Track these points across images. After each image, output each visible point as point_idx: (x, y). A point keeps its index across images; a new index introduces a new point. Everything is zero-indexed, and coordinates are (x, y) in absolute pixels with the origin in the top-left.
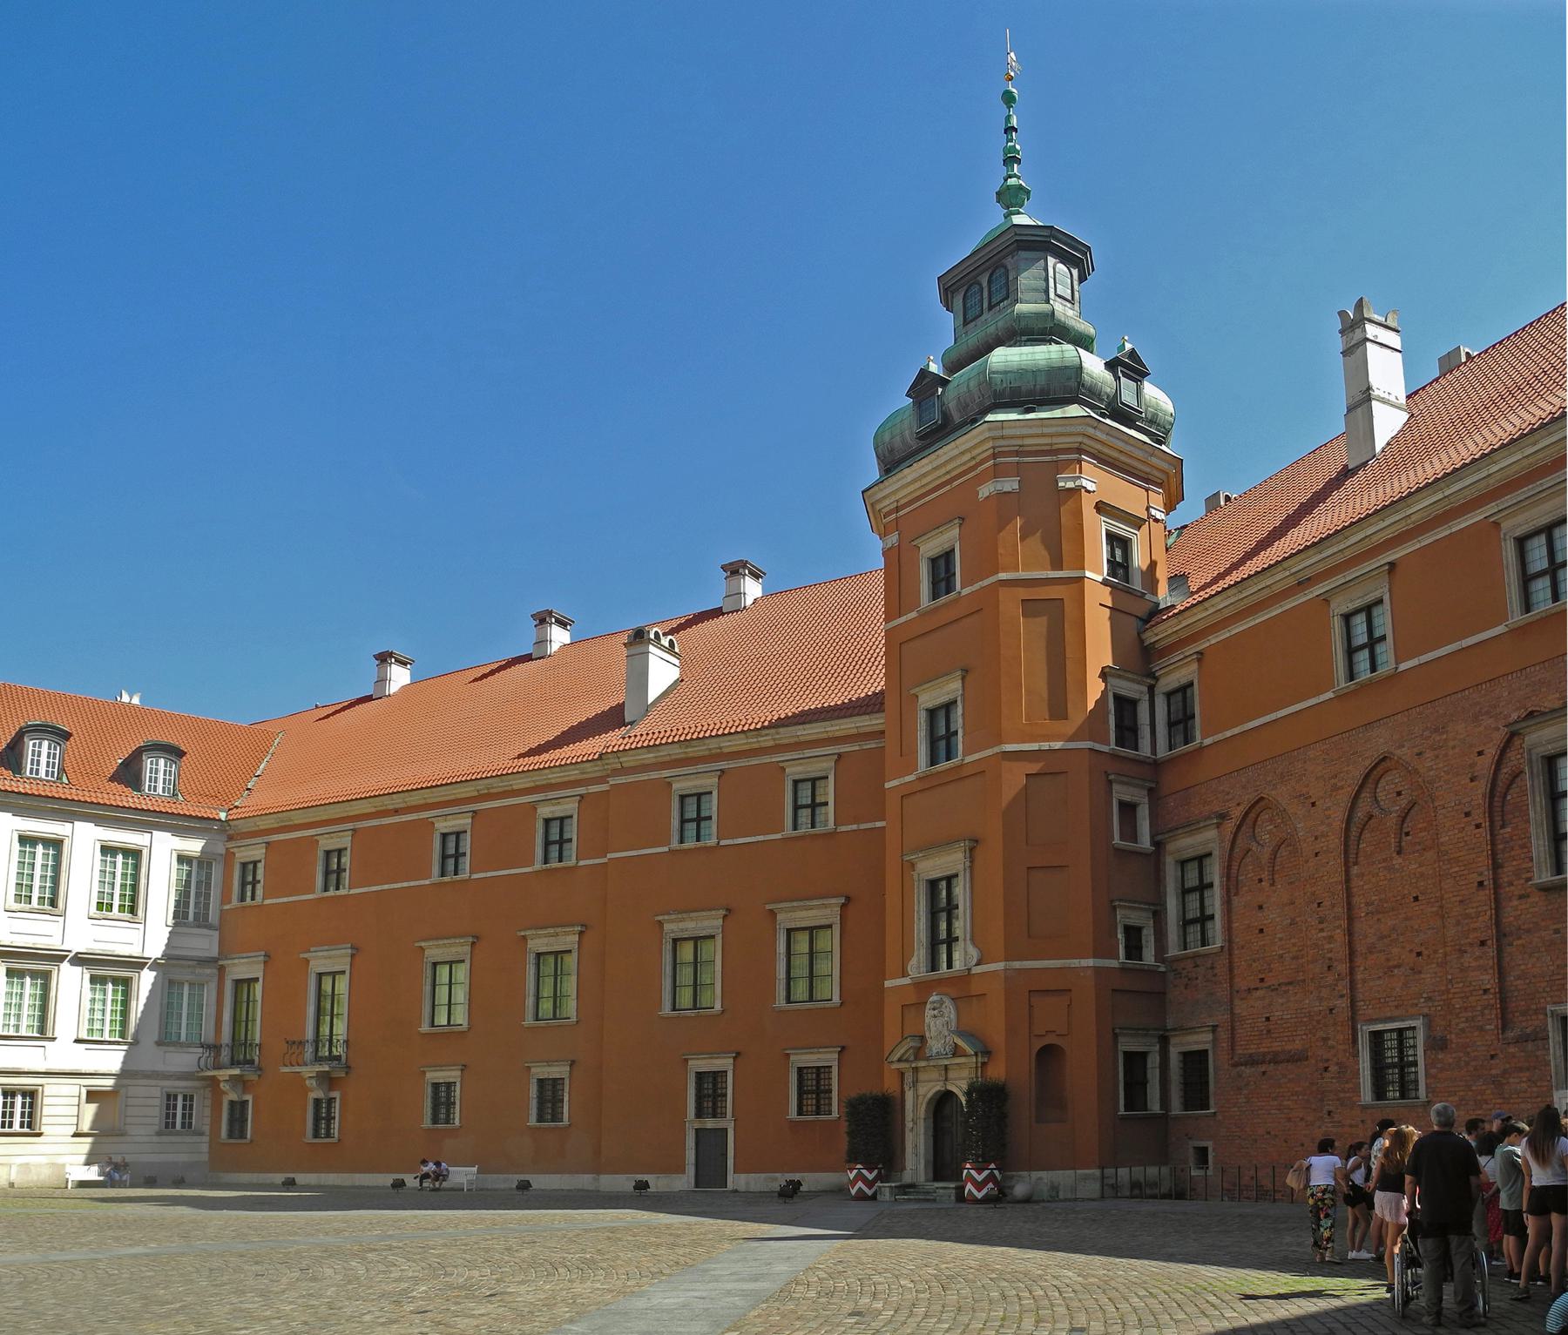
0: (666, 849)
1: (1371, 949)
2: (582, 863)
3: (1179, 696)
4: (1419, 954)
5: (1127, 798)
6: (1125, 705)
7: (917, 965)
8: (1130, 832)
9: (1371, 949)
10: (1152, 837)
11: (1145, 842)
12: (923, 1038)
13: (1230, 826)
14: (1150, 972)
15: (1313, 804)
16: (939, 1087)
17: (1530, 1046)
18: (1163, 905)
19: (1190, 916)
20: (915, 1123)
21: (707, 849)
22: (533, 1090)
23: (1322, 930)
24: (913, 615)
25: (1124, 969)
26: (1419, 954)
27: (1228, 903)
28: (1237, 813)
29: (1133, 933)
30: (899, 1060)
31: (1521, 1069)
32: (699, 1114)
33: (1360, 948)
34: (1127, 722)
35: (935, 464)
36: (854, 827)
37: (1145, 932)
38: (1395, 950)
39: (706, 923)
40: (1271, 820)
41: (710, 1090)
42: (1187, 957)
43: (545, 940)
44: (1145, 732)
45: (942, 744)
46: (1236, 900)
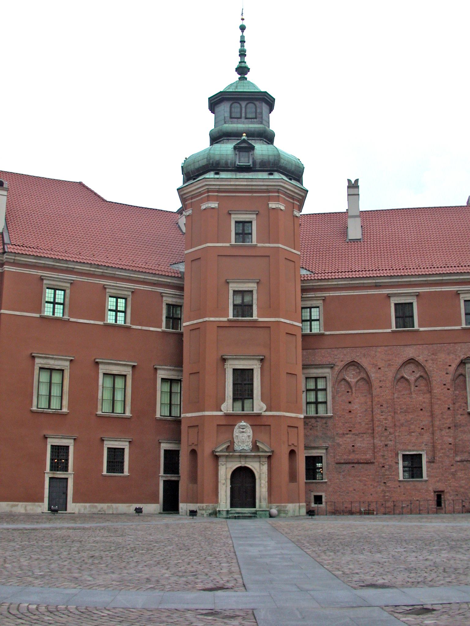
1: (402, 425)
4: (422, 429)
9: (402, 425)
13: (337, 369)
15: (379, 368)
17: (465, 463)
23: (382, 415)
26: (422, 429)
27: (333, 398)
28: (341, 365)
31: (462, 470)
33: (397, 424)
36: (139, 327)
38: (412, 427)
40: (354, 370)
46: (337, 398)
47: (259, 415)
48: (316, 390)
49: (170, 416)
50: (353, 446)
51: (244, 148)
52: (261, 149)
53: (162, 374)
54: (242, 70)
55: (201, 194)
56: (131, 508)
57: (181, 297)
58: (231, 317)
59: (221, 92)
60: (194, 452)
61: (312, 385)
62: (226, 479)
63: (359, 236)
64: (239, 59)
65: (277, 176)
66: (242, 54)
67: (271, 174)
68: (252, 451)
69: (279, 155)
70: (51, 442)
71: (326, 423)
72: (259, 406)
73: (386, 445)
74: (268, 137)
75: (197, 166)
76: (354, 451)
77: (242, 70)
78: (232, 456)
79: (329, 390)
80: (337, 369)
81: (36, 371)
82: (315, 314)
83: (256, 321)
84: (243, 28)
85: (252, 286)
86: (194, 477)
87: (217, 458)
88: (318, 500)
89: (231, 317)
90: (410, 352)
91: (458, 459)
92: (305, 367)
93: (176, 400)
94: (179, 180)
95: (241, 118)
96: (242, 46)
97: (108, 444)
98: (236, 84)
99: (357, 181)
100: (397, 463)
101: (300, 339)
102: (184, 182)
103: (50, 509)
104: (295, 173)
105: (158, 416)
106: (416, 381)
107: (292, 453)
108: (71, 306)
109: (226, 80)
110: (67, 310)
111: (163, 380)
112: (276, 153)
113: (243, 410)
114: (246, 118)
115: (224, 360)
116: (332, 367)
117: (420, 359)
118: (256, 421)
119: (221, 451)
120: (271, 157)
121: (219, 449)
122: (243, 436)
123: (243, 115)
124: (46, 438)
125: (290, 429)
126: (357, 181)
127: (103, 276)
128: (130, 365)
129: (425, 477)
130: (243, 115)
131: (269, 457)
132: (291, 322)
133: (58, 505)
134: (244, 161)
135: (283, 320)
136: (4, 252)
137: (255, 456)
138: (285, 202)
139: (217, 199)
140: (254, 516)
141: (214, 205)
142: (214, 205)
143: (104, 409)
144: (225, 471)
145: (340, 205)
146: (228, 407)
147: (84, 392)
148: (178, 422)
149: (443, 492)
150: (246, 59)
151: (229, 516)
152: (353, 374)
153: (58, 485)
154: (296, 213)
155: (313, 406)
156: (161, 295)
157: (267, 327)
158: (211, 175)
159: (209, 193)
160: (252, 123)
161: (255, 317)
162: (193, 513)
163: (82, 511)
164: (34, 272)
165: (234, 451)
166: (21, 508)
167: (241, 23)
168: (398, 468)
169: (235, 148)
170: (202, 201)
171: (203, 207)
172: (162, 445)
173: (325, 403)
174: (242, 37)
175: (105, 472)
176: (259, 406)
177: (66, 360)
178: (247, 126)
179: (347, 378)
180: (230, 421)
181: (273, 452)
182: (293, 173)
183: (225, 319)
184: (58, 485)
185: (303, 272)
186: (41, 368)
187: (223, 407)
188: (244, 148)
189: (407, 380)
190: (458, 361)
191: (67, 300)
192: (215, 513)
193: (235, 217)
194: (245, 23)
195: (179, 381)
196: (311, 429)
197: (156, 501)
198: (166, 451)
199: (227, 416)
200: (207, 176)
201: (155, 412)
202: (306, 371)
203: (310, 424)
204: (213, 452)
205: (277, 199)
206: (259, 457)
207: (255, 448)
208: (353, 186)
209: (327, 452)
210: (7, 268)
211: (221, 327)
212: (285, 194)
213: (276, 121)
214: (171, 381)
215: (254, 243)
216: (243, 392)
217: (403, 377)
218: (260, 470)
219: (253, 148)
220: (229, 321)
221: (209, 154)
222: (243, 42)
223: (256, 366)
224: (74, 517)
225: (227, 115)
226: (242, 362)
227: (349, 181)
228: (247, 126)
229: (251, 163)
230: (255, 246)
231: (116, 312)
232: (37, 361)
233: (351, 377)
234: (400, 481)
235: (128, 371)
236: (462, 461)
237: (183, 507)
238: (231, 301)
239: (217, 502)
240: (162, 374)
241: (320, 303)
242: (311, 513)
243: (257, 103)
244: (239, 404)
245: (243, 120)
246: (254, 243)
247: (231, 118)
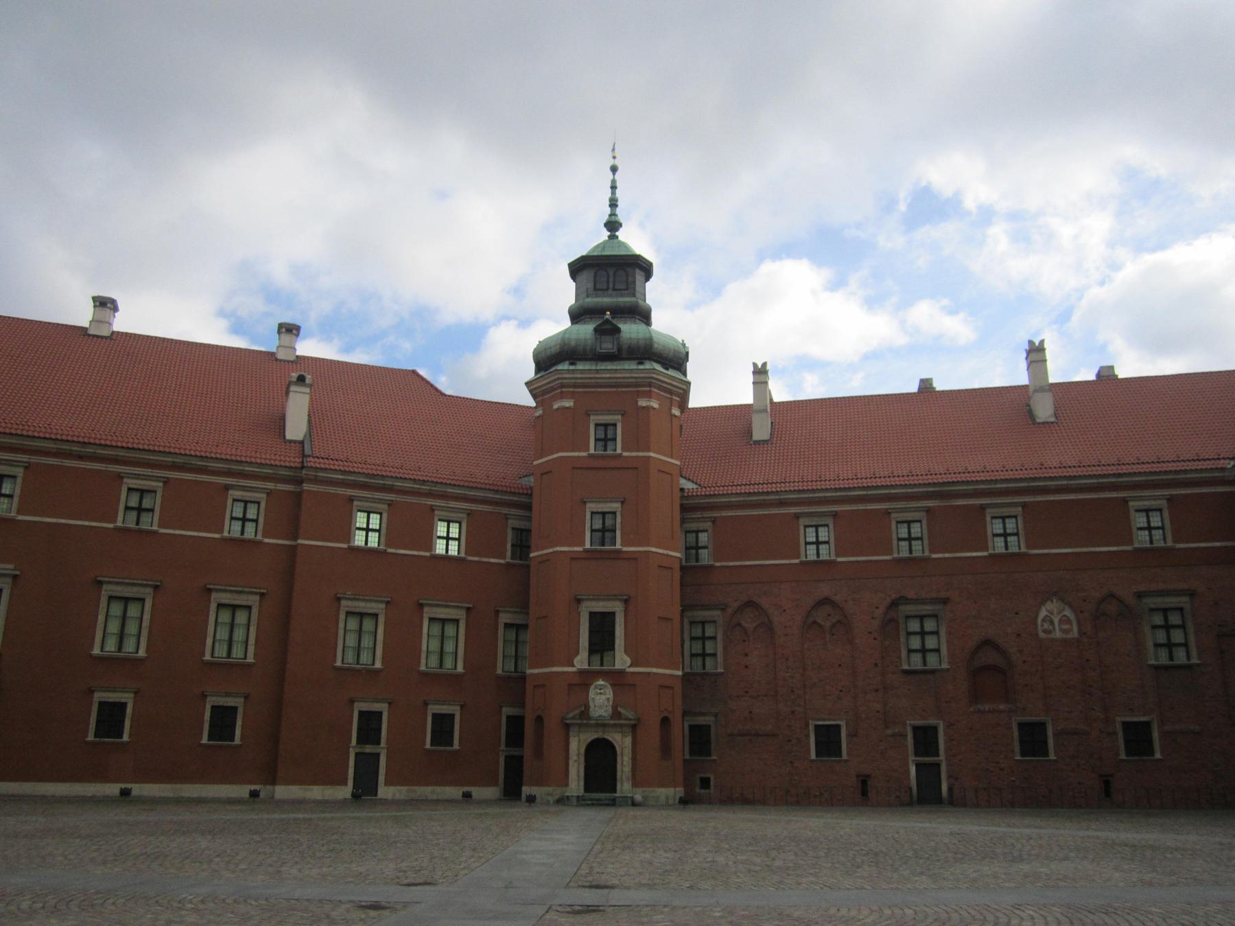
27: (725, 648)
28: (736, 605)
36: (476, 559)
47: (622, 673)
48: (703, 639)
49: (516, 671)
51: (607, 330)
52: (630, 330)
53: (504, 618)
54: (613, 226)
55: (553, 389)
56: (455, 792)
57: (529, 519)
58: (588, 546)
59: (583, 258)
60: (539, 719)
61: (697, 632)
62: (578, 755)
63: (766, 436)
64: (608, 210)
65: (648, 365)
66: (613, 204)
68: (612, 718)
69: (651, 339)
70: (359, 706)
72: (621, 660)
73: (793, 712)
74: (644, 316)
75: (549, 353)
77: (613, 226)
78: (587, 725)
79: (720, 637)
80: (730, 610)
81: (342, 616)
82: (703, 538)
83: (619, 551)
84: (614, 169)
85: (616, 506)
86: (538, 752)
87: (567, 726)
88: (705, 783)
89: (588, 546)
90: (824, 590)
91: (889, 732)
92: (685, 608)
93: (526, 651)
94: (530, 372)
96: (613, 193)
97: (434, 709)
98: (603, 245)
99: (765, 364)
100: (808, 736)
101: (677, 575)
102: (536, 373)
103: (353, 795)
104: (676, 360)
105: (499, 671)
106: (834, 625)
107: (665, 721)
108: (390, 533)
109: (591, 239)
110: (383, 539)
111: (507, 626)
112: (647, 335)
113: (602, 664)
114: (614, 289)
115: (579, 601)
116: (723, 609)
117: (837, 598)
118: (618, 679)
119: (573, 718)
120: (641, 342)
121: (571, 715)
122: (601, 699)
123: (611, 285)
124: (352, 701)
126: (765, 364)
127: (430, 494)
129: (845, 756)
130: (611, 285)
131: (634, 727)
132: (665, 552)
133: (365, 789)
134: (607, 346)
135: (654, 549)
136: (303, 467)
137: (615, 725)
138: (658, 398)
139: (572, 395)
140: (613, 803)
141: (569, 403)
142: (569, 403)
143: (428, 663)
144: (577, 745)
145: (743, 395)
146: (581, 661)
147: (403, 643)
148: (523, 678)
149: (868, 776)
150: (618, 211)
151: (581, 802)
153: (367, 765)
154: (676, 412)
155: (700, 660)
156: (506, 517)
157: (633, 558)
158: (564, 366)
159: (561, 389)
160: (622, 296)
161: (618, 546)
162: (531, 799)
163: (398, 796)
164: (340, 491)
165: (589, 718)
166: (316, 792)
167: (611, 162)
168: (809, 744)
169: (595, 330)
170: (555, 398)
171: (556, 406)
172: (504, 709)
173: (714, 655)
174: (614, 181)
175: (428, 746)
177: (382, 602)
178: (615, 300)
179: (743, 623)
180: (585, 679)
181: (639, 719)
182: (671, 361)
183: (580, 549)
184: (367, 765)
185: (688, 486)
187: (576, 660)
188: (607, 330)
189: (820, 626)
190: (889, 600)
191: (384, 525)
192: (562, 801)
193: (594, 419)
194: (617, 162)
195: (525, 627)
197: (495, 784)
198: (508, 717)
199: (581, 672)
200: (560, 367)
201: (495, 666)
202: (689, 614)
204: (563, 719)
205: (648, 395)
206: (621, 726)
207: (616, 714)
208: (760, 373)
210: (306, 486)
211: (574, 558)
212: (660, 388)
213: (654, 293)
214: (520, 628)
215: (619, 451)
216: (602, 640)
217: (814, 622)
218: (623, 743)
219: (618, 330)
220: (586, 551)
221: (563, 339)
222: (614, 188)
223: (617, 607)
224: (384, 802)
225: (591, 285)
226: (601, 604)
227: (755, 365)
228: (615, 300)
229: (615, 350)
231: (447, 540)
232: (343, 603)
233: (749, 621)
234: (812, 761)
235: (461, 615)
236: (893, 735)
237: (526, 790)
238: (588, 525)
239: (567, 785)
240: (504, 618)
241: (708, 525)
242: (684, 802)
243: (629, 270)
244: (597, 658)
245: (610, 292)
246: (619, 451)
247: (595, 289)
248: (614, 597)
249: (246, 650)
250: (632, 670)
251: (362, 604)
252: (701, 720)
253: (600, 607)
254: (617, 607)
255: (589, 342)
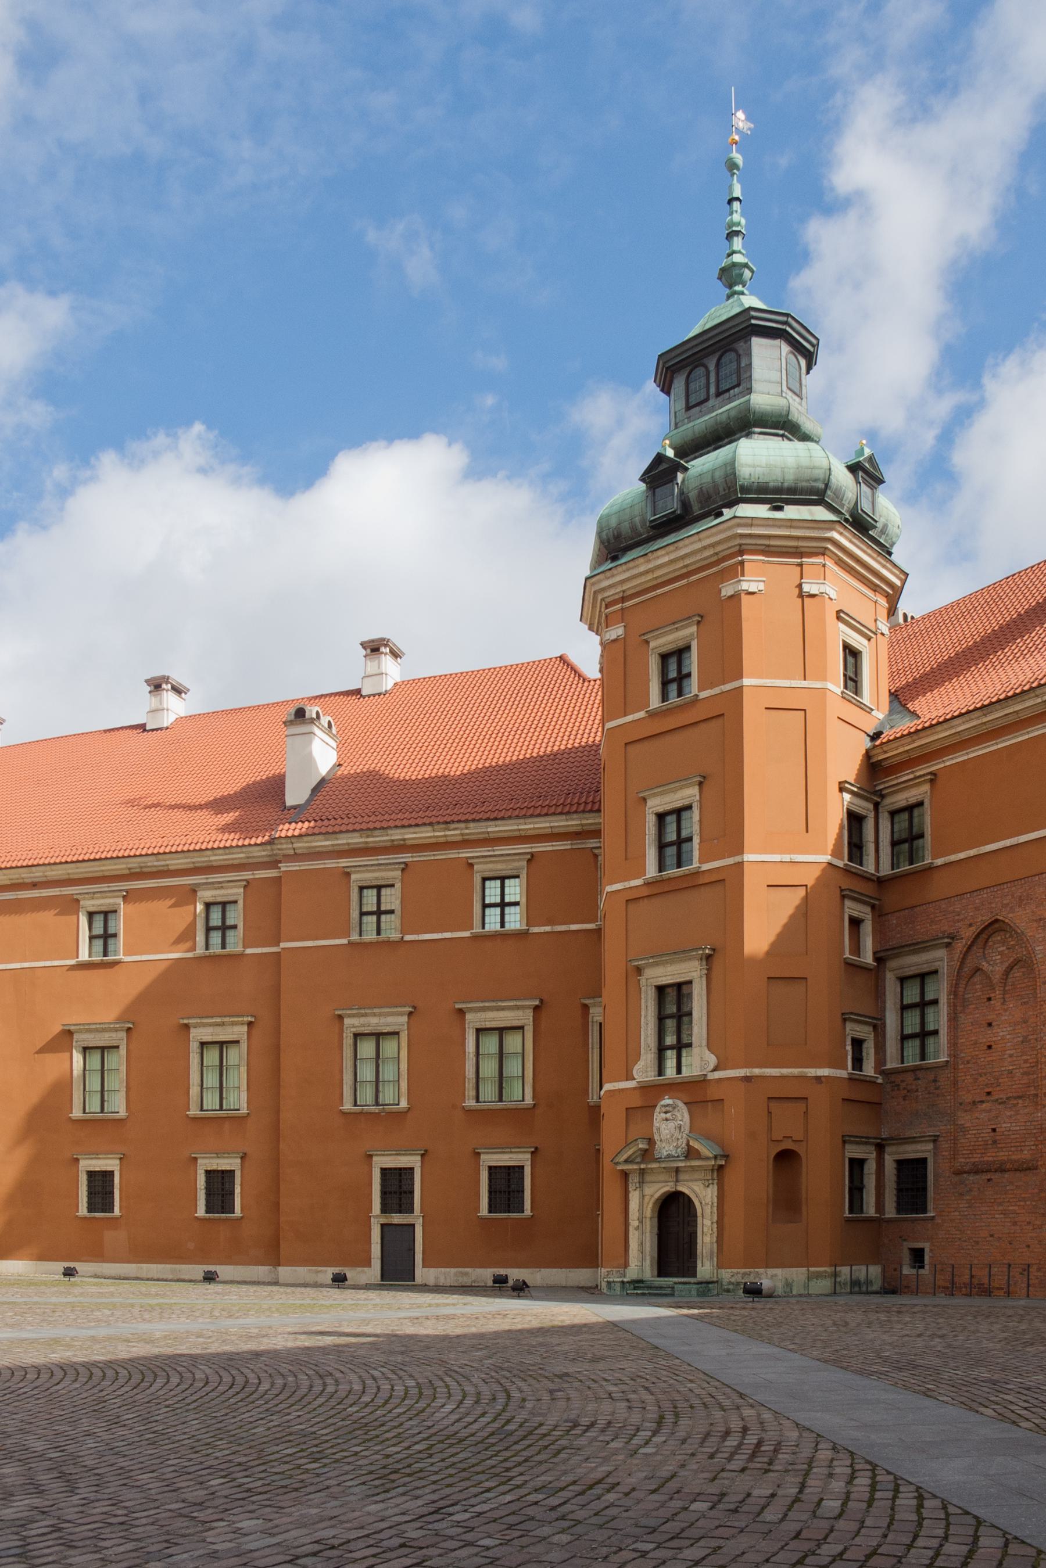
0: (345, 941)
2: (249, 951)
3: (905, 816)
5: (855, 914)
6: (854, 819)
7: (644, 1070)
8: (856, 949)
10: (874, 953)
11: (868, 958)
12: (651, 1141)
14: (869, 1082)
16: (668, 1188)
18: (882, 1019)
19: (908, 1031)
20: (641, 1222)
21: (388, 943)
22: (201, 1181)
24: (642, 714)
25: (851, 1079)
29: (858, 1044)
30: (626, 1161)
32: (385, 1209)
34: (855, 840)
35: (672, 556)
37: (865, 1045)
39: (390, 1019)
41: (397, 1188)
42: (905, 1071)
43: (210, 1030)
44: (870, 848)
45: (671, 851)
50: (994, 1130)
67: (780, 509)
71: (935, 1081)
76: (995, 1142)
81: (348, 1041)
95: (706, 400)
116: (948, 945)
123: (713, 390)
125: (772, 1104)
128: (528, 1007)
152: (1001, 953)
176: (699, 1061)
186: (356, 1036)
196: (905, 1098)
203: (903, 1085)
209: (935, 1148)
230: (696, 699)
232: (347, 1021)
248: (681, 954)
249: (239, 1100)
250: (717, 1075)
251: (374, 1020)
252: (911, 1152)
253: (668, 974)
254: (690, 970)
255: (637, 511)
